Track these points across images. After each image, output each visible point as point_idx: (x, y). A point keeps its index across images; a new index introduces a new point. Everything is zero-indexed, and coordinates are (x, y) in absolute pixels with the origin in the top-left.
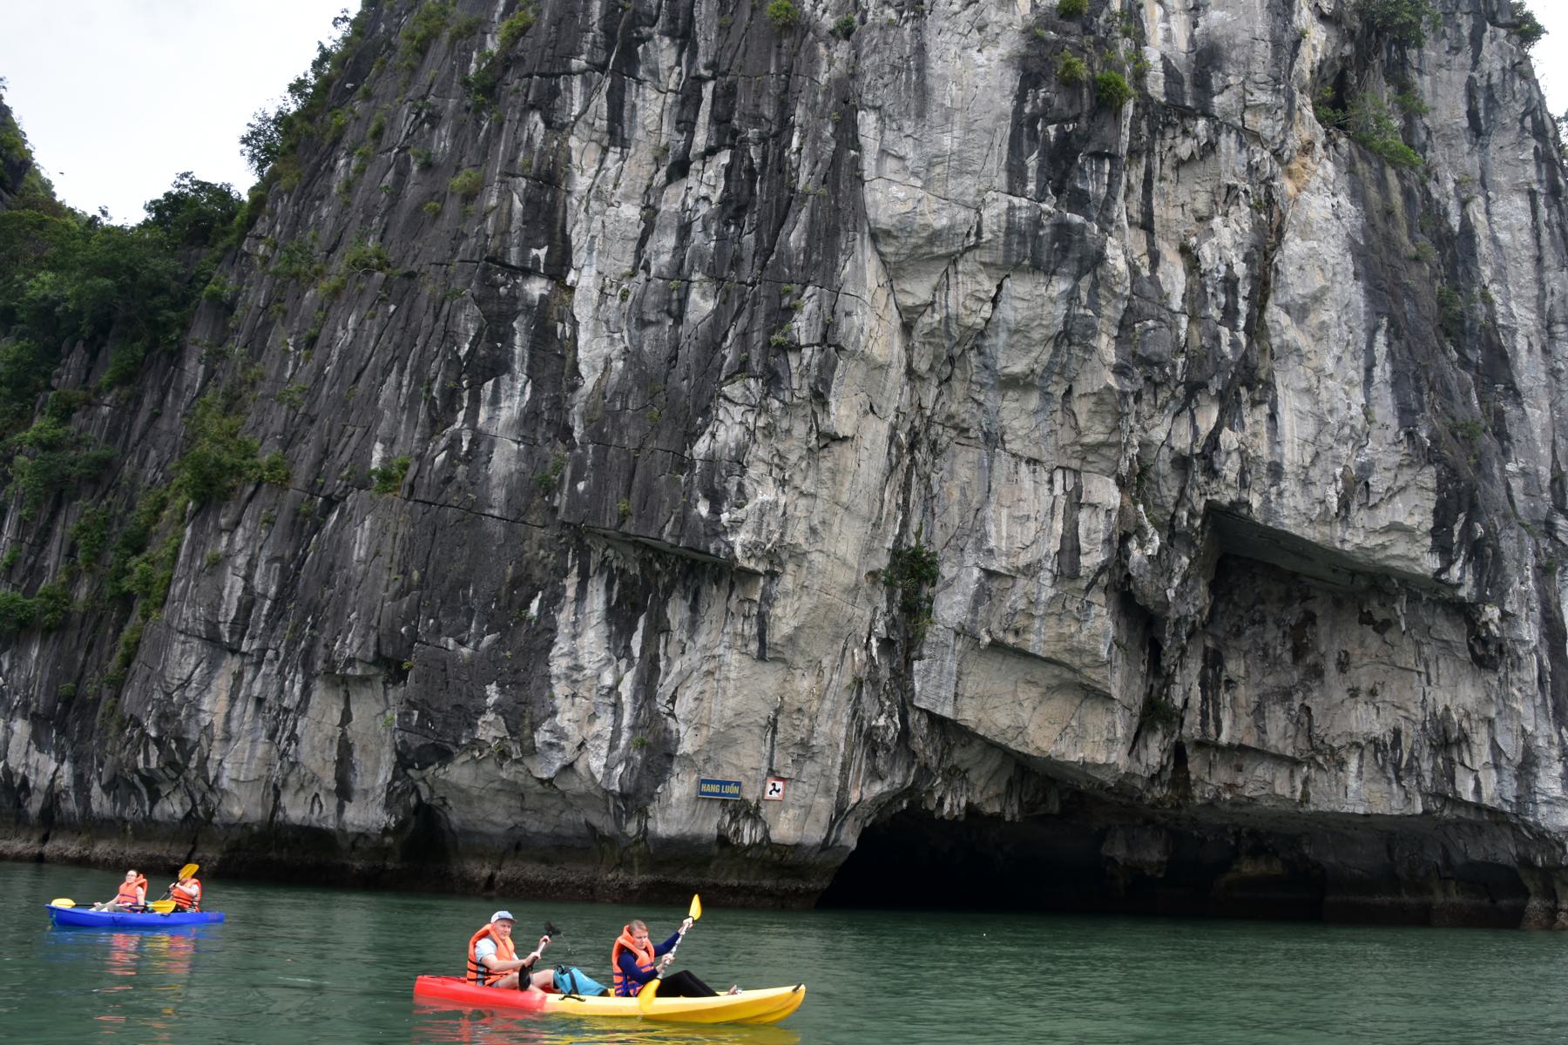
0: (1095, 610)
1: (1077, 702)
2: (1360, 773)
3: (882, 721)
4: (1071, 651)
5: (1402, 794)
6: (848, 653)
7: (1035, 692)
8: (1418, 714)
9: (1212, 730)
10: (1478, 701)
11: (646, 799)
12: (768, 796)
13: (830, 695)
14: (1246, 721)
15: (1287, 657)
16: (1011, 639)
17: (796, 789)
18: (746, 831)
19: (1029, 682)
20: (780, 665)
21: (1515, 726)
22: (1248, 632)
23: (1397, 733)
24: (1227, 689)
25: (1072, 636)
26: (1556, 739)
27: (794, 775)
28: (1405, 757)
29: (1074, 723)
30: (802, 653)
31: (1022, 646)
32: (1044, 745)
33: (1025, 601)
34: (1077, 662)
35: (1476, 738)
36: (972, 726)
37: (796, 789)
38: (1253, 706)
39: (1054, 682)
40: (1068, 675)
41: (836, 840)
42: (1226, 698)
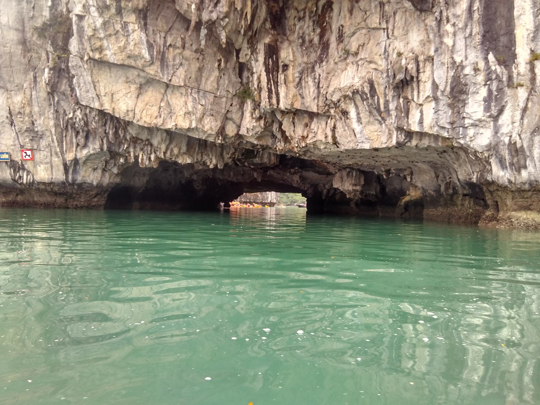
0: (131, 27)
1: (163, 91)
2: (359, 120)
3: (71, 115)
4: (129, 57)
5: (387, 131)
7: (133, 87)
8: (382, 64)
9: (274, 101)
10: (423, 44)
13: (35, 103)
14: (293, 91)
15: (316, 40)
16: (97, 56)
17: (40, 154)
18: (25, 177)
19: (127, 82)
21: (446, 59)
22: (297, 27)
23: (371, 84)
24: (284, 71)
25: (125, 48)
26: (482, 65)
27: (35, 147)
28: (382, 101)
29: (162, 104)
30: (9, 81)
31: (105, 59)
32: (148, 120)
33: (90, 30)
34: (140, 63)
35: (423, 77)
36: (111, 113)
38: (297, 80)
39: (142, 81)
40: (142, 74)
41: (74, 180)
42: (281, 77)
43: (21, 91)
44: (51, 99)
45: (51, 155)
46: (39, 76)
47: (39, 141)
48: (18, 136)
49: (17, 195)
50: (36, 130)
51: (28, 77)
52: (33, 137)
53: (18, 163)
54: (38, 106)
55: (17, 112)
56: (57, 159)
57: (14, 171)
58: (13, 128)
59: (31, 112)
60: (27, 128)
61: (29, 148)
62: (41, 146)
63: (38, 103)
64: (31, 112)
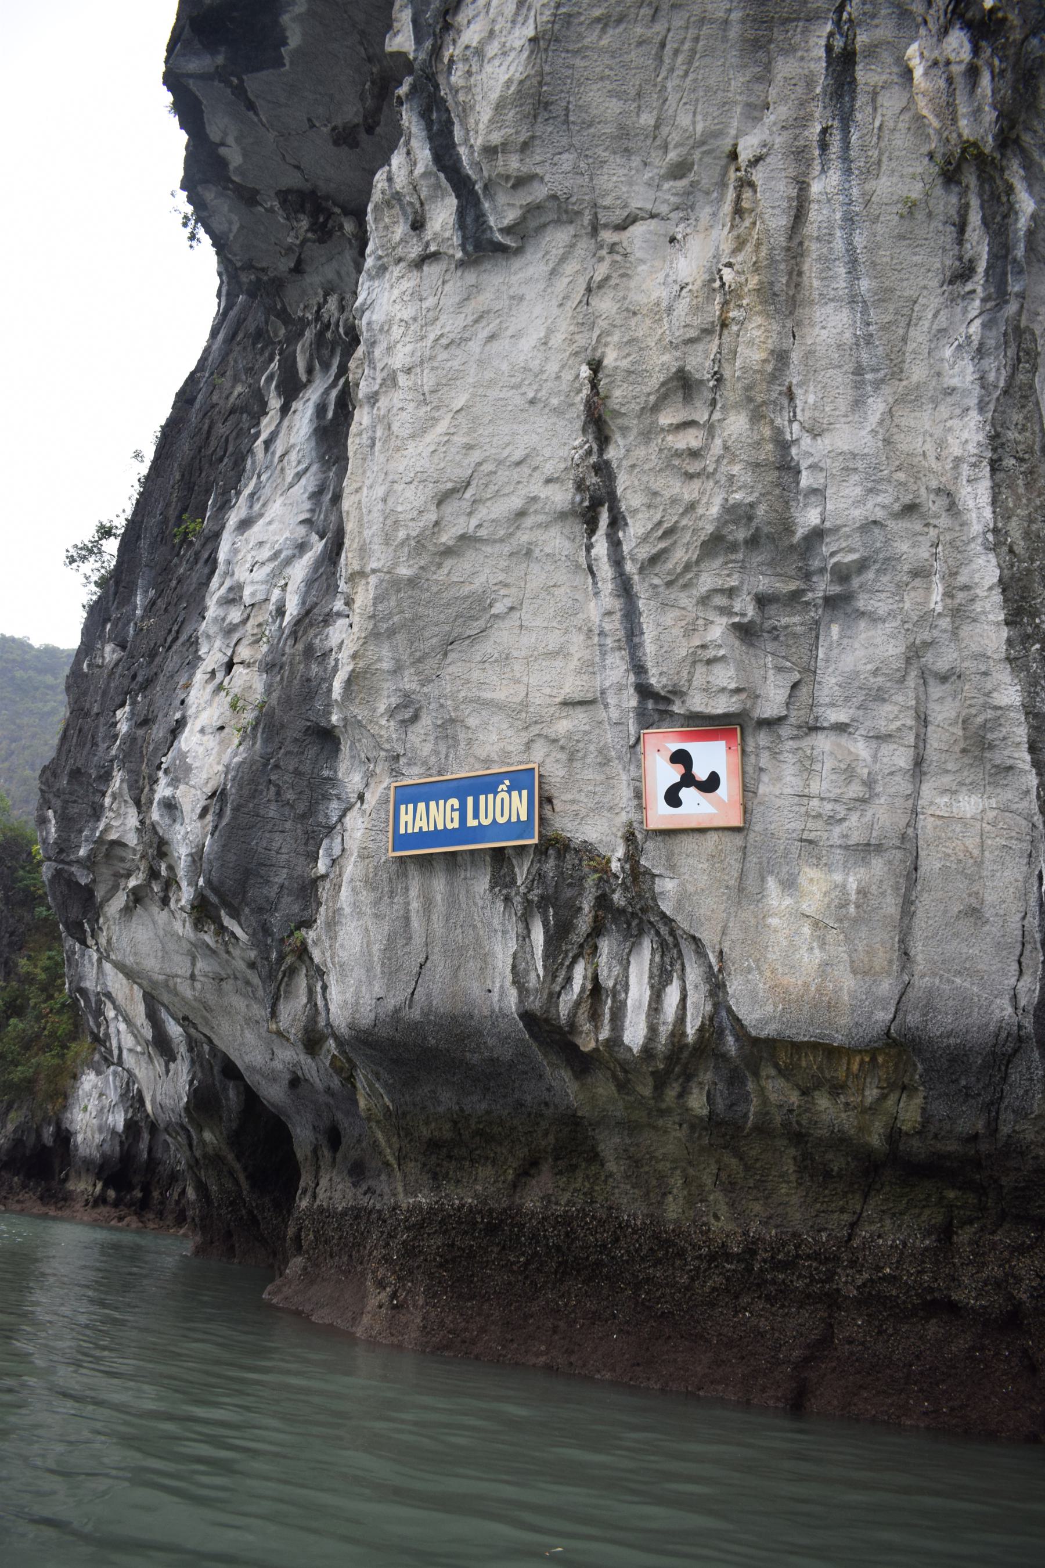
6: (865, 75)
11: (289, 906)
12: (660, 815)
17: (807, 766)
18: (638, 992)
20: (558, 238)
37: (807, 766)
43: (704, 213)
44: (975, 218)
45: (919, 762)
46: (872, 51)
47: (816, 626)
48: (631, 617)
49: (529, 1168)
50: (809, 517)
51: (785, 68)
52: (762, 601)
53: (604, 869)
54: (853, 299)
55: (655, 381)
56: (969, 805)
57: (556, 938)
58: (601, 547)
59: (781, 357)
60: (735, 514)
61: (721, 706)
62: (829, 683)
63: (853, 263)
64: (781, 357)
